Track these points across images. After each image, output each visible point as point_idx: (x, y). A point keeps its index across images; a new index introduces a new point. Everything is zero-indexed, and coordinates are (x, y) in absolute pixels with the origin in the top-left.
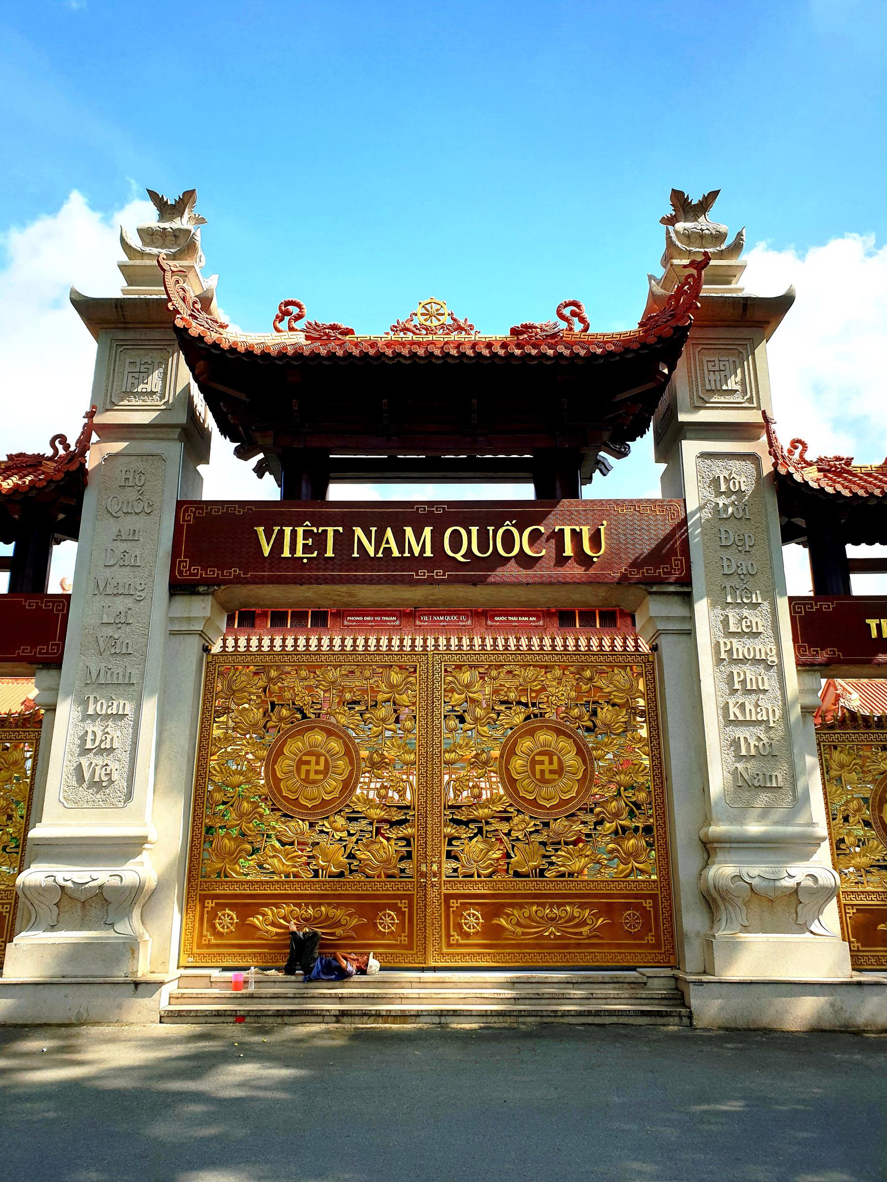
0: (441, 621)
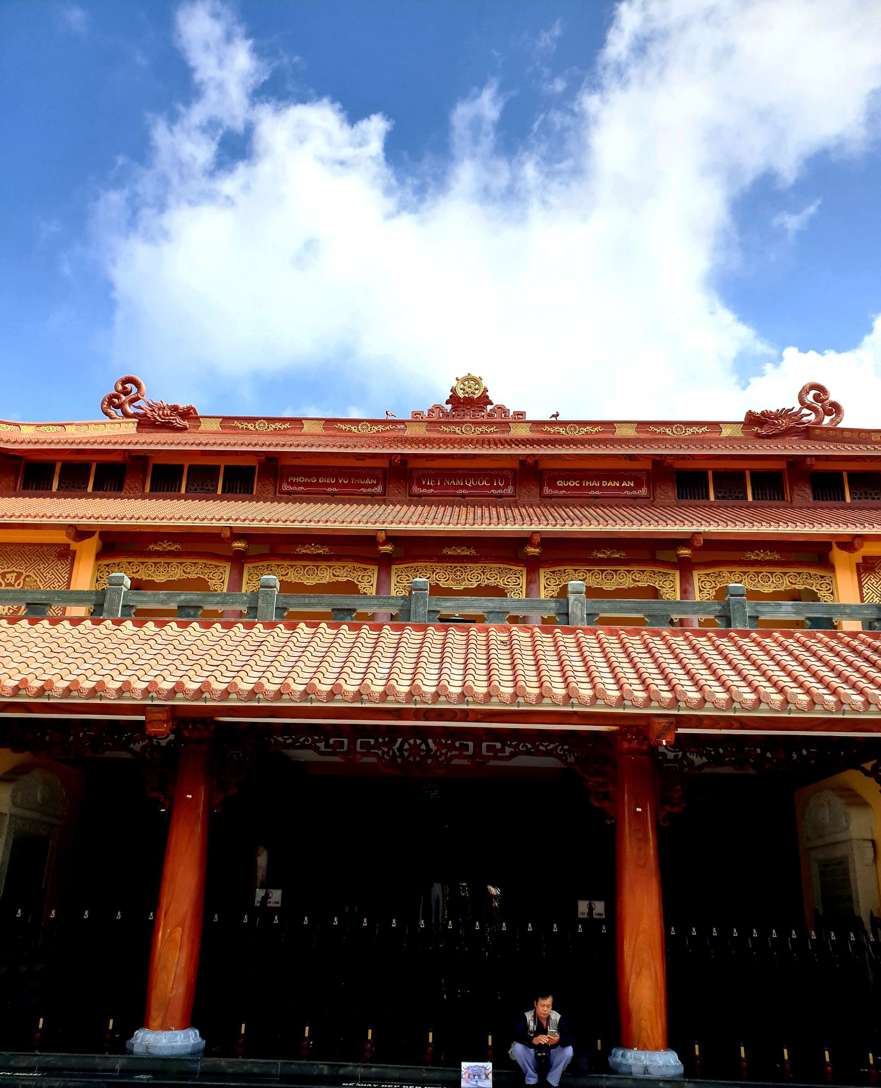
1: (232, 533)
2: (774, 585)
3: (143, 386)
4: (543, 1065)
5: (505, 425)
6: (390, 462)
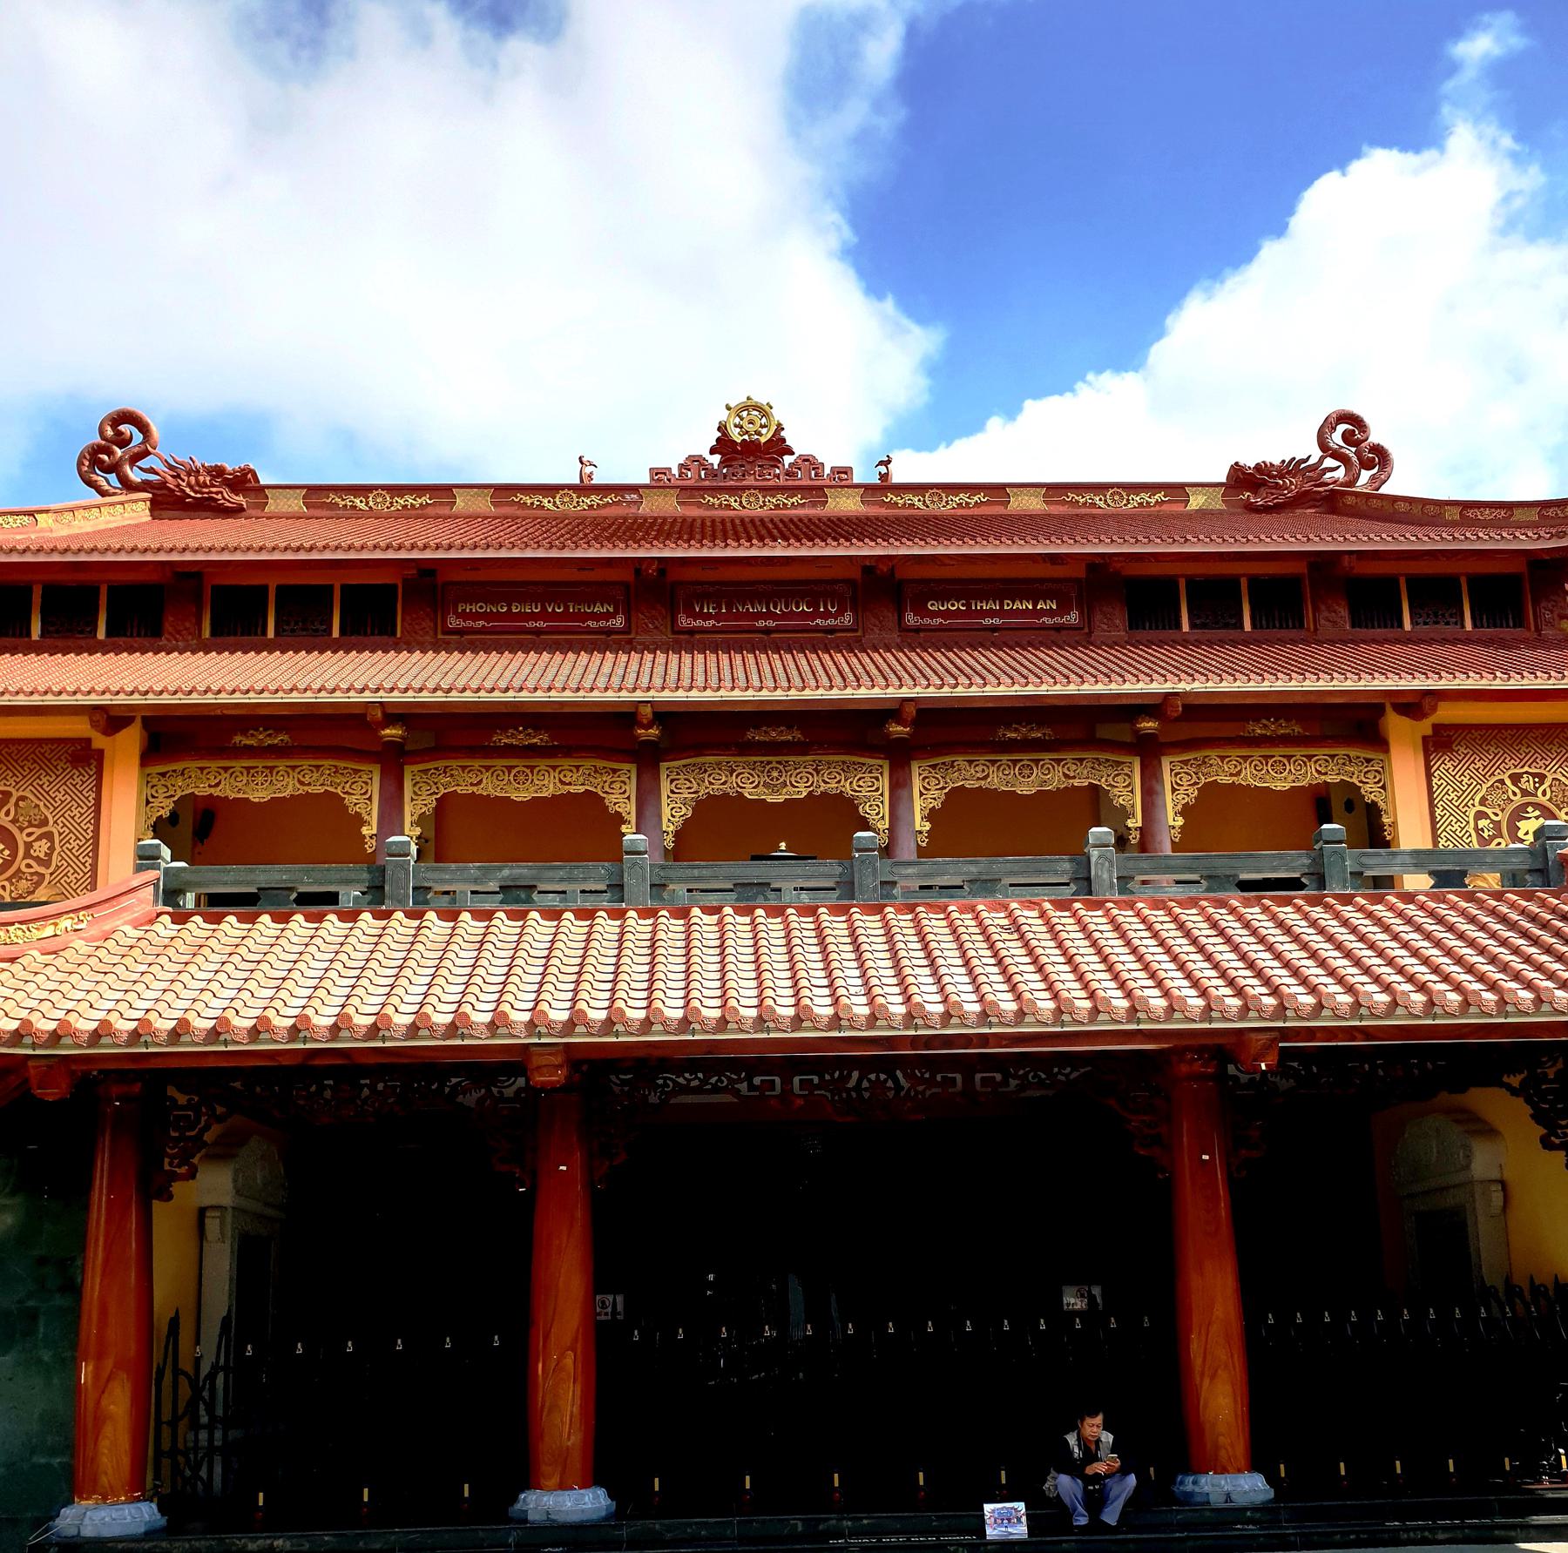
0: (759, 616)
1: (385, 714)
2: (1292, 777)
3: (154, 428)
4: (1095, 1501)
5: (816, 492)
6: (638, 572)
